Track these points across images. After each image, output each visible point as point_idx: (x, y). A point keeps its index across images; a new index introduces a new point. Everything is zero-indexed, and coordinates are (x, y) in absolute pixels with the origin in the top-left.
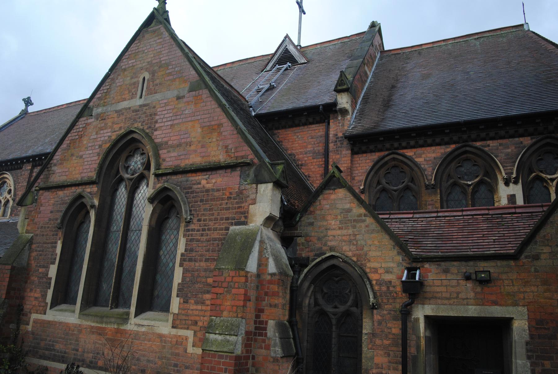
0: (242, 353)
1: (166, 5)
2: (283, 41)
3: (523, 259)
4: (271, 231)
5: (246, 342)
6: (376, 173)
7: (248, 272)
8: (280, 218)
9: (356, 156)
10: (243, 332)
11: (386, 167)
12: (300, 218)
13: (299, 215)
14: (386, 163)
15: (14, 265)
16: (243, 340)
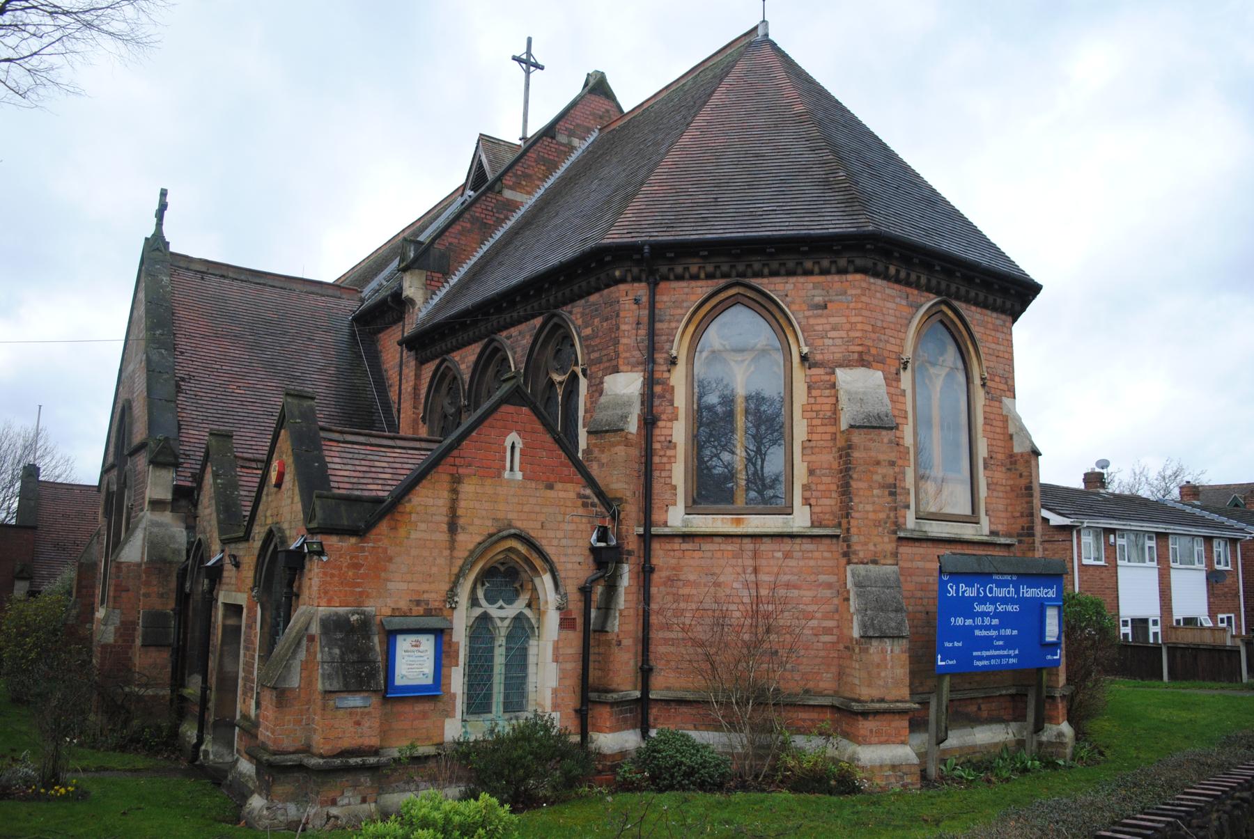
0: (115, 641)
1: (149, 236)
2: (476, 151)
3: (251, 541)
4: (171, 514)
5: (122, 631)
6: (435, 391)
7: (122, 563)
8: (173, 499)
9: (423, 367)
10: (118, 622)
11: (447, 381)
12: (198, 495)
13: (196, 492)
14: (444, 376)
15: (82, 561)
16: (117, 630)
